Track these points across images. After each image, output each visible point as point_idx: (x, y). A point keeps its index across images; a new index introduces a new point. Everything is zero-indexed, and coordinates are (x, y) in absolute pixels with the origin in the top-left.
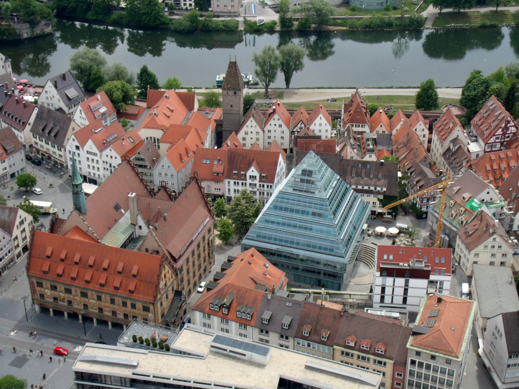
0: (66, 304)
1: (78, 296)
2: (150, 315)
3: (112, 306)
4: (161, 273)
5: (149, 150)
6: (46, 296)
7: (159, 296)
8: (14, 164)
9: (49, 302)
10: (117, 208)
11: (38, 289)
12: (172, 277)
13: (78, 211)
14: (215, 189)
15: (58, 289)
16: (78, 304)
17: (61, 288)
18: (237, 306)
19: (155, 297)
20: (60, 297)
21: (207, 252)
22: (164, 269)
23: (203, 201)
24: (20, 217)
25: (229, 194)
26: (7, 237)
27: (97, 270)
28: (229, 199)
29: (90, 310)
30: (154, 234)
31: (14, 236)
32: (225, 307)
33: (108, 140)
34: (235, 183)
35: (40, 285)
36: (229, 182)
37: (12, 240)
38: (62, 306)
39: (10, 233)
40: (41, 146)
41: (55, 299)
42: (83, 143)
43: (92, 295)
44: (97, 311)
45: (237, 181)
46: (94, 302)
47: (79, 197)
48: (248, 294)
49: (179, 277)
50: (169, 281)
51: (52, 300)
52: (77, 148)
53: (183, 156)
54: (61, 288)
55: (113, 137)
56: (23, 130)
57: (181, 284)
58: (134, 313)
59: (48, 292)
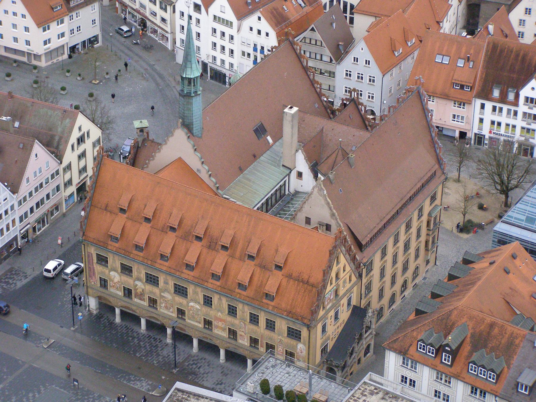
0: (146, 303)
1: (168, 292)
3: (230, 319)
4: (330, 267)
5: (332, 24)
7: (321, 313)
8: (79, 28)
9: (115, 296)
10: (260, 131)
11: (98, 268)
12: (350, 280)
13: (186, 130)
14: (454, 116)
15: (135, 273)
16: (166, 307)
17: (140, 273)
19: (314, 313)
21: (423, 238)
22: (338, 263)
23: (429, 137)
24: (80, 129)
25: (480, 129)
26: (53, 164)
27: (209, 247)
28: (480, 139)
29: (188, 321)
30: (325, 192)
31: (65, 163)
32: (447, 352)
35: (102, 260)
36: (483, 106)
37: (61, 172)
38: (138, 306)
39: (59, 156)
41: (128, 293)
43: (195, 293)
44: (201, 326)
45: (498, 105)
46: (198, 307)
47: (191, 104)
48: (496, 330)
49: (364, 280)
50: (344, 287)
51: (121, 293)
52: (197, 7)
53: (397, 44)
54: (139, 271)
58: (271, 339)
59: (115, 277)
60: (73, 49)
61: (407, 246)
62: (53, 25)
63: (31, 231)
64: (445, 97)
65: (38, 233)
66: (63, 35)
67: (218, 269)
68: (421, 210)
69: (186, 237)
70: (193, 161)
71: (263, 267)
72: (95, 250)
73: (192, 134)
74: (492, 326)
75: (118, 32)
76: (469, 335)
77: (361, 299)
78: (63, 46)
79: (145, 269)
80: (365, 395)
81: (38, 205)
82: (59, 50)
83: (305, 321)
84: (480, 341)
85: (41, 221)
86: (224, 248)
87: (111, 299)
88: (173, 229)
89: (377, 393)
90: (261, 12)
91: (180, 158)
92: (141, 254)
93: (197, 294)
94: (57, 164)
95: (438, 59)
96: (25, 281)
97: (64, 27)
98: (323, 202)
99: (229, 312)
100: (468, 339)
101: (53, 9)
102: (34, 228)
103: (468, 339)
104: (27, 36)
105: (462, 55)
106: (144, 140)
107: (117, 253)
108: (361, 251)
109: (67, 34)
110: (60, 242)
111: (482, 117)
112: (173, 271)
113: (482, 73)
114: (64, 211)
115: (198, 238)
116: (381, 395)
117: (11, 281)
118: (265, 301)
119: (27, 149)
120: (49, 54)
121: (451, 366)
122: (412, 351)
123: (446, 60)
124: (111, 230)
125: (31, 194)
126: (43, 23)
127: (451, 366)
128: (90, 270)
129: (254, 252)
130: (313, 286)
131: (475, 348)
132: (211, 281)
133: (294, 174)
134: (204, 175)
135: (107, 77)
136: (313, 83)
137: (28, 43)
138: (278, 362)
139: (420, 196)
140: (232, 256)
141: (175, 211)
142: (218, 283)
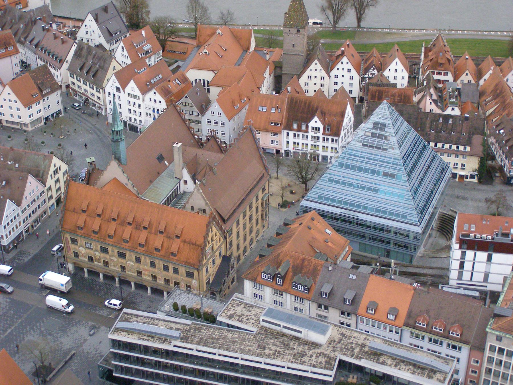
0: (102, 264)
2: (194, 281)
3: (152, 269)
4: (207, 234)
6: (81, 255)
7: (205, 261)
8: (49, 106)
9: (84, 262)
10: (161, 158)
11: (72, 246)
12: (220, 241)
13: (117, 161)
14: (272, 141)
16: (114, 266)
17: (97, 247)
18: (293, 277)
19: (200, 261)
20: (95, 257)
21: (260, 213)
22: (212, 231)
24: (55, 165)
25: (288, 147)
26: (41, 187)
27: (136, 228)
28: (288, 153)
31: (48, 186)
32: (279, 277)
33: (152, 81)
35: (74, 241)
37: (46, 191)
38: (98, 266)
39: (44, 183)
40: (79, 87)
41: (91, 259)
42: (124, 84)
43: (130, 256)
44: (135, 274)
45: (297, 133)
47: (119, 146)
48: (306, 263)
49: (228, 240)
50: (216, 245)
51: (87, 260)
52: (118, 89)
53: (236, 102)
55: (158, 78)
57: (230, 249)
58: (176, 279)
60: (47, 119)
61: (251, 219)
62: (34, 106)
63: (30, 227)
64: (266, 130)
65: (35, 229)
66: (40, 111)
67: (142, 241)
68: (257, 197)
69: (122, 223)
70: (123, 179)
71: (169, 237)
73: (121, 163)
74: (303, 260)
75: (73, 107)
76: (291, 267)
78: (41, 117)
80: (234, 307)
81: (33, 212)
82: (39, 120)
83: (196, 267)
84: (298, 269)
85: (36, 221)
86: (145, 228)
87: (81, 263)
88: (114, 220)
89: (241, 305)
90: (156, 89)
91: (115, 178)
92: (97, 236)
93: (132, 256)
94: (42, 187)
95: (260, 109)
96: (29, 258)
97: (41, 106)
98: (200, 197)
99: (151, 265)
100: (291, 270)
101: (33, 96)
102: (32, 226)
103: (291, 270)
104: (19, 113)
105: (274, 106)
106: (93, 169)
107: (82, 236)
108: (225, 223)
110: (48, 232)
111: (288, 140)
112: (116, 244)
113: (286, 115)
114: (49, 214)
115: (130, 224)
116: (243, 306)
117: (21, 258)
118: (171, 257)
119: (24, 180)
120: (33, 123)
121: (282, 285)
122: (259, 278)
123: (265, 109)
124: (78, 223)
125: (29, 206)
126: (28, 105)
127: (282, 285)
128: (67, 248)
129: (162, 229)
130: (198, 246)
131: (295, 274)
132: (139, 248)
133: (182, 182)
134: (130, 187)
135: (68, 134)
136: (189, 128)
137: (20, 117)
138: (182, 292)
139: (256, 189)
140: (150, 232)
141: (115, 209)
142: (143, 249)
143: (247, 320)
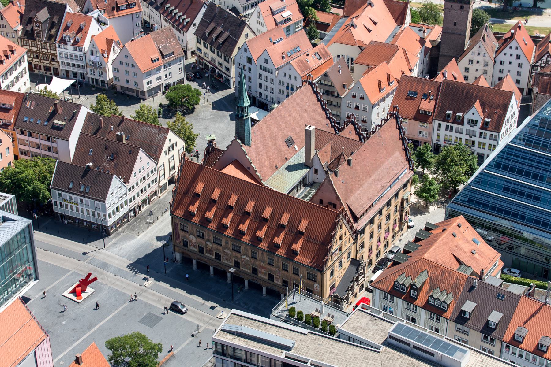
0: (213, 257)
2: (316, 285)
3: (269, 267)
5: (339, 71)
9: (193, 252)
11: (181, 233)
16: (227, 259)
20: (207, 247)
24: (170, 140)
26: (153, 165)
29: (241, 268)
34: (447, 126)
36: (440, 125)
38: (209, 258)
40: (205, 54)
41: (201, 250)
44: (250, 271)
45: (450, 124)
51: (196, 250)
56: (186, 32)
59: (193, 239)
72: (180, 221)
77: (357, 253)
78: (160, 85)
79: (213, 234)
81: (142, 191)
87: (190, 254)
93: (248, 251)
109: (163, 78)
125: (137, 184)
128: (176, 235)
137: (136, 84)
143: (373, 335)
